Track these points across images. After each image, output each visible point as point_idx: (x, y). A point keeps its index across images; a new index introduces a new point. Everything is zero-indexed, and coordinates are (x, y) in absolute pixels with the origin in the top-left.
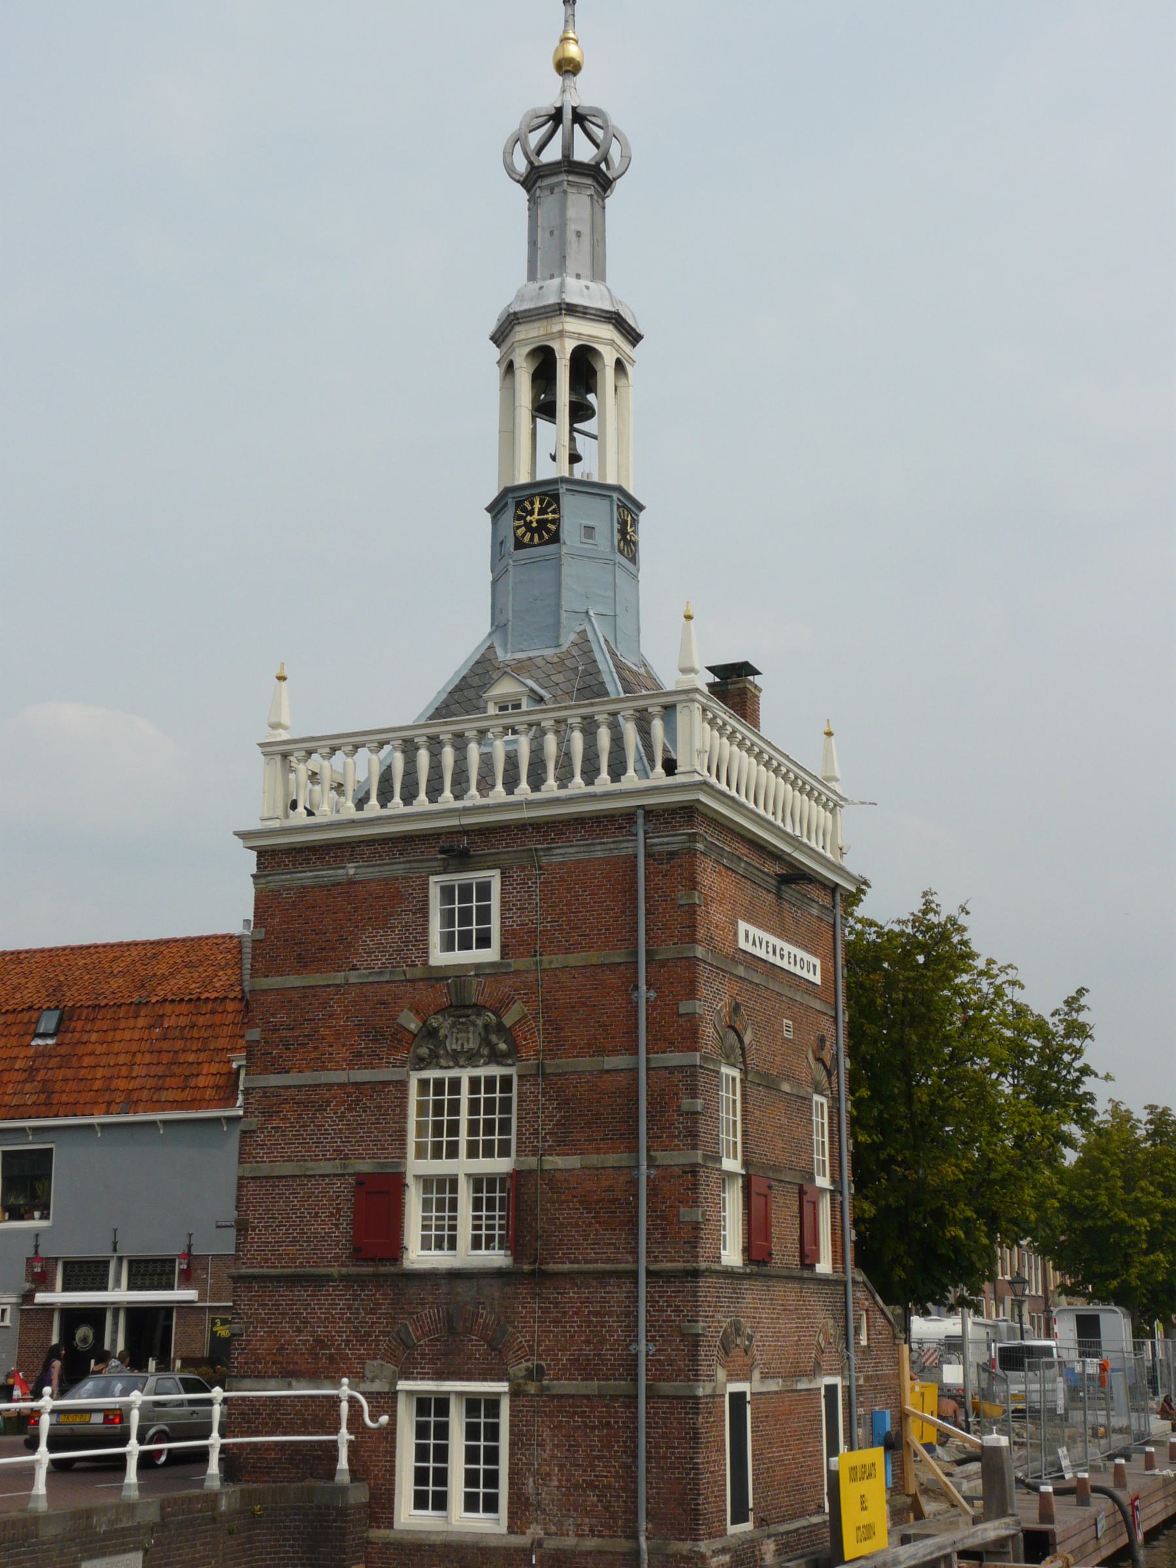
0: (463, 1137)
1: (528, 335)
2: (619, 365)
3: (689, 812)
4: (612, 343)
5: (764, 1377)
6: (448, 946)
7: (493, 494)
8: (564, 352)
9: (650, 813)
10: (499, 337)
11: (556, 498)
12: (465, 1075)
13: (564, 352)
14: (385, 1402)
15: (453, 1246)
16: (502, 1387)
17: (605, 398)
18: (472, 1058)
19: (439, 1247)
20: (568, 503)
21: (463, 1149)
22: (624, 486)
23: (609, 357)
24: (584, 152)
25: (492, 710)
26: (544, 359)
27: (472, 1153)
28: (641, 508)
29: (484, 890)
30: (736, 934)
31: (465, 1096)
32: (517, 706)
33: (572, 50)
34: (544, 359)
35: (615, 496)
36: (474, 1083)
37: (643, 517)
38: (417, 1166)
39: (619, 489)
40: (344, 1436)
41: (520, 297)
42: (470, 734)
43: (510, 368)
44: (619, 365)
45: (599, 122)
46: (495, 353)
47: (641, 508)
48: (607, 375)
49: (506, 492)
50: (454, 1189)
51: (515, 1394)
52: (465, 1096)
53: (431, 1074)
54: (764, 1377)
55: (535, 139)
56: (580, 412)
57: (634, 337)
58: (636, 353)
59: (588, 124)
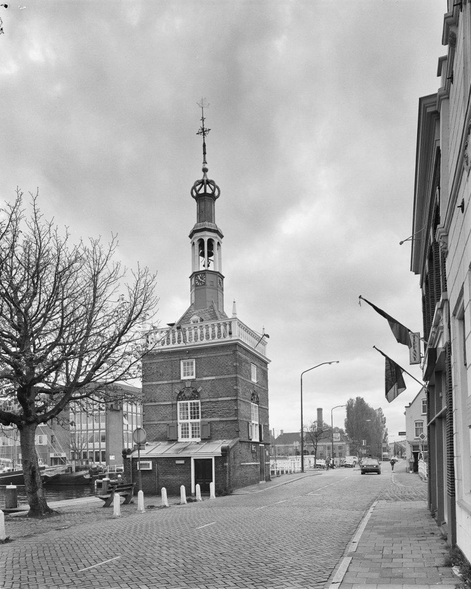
0: (189, 415)
1: (198, 235)
2: (219, 244)
3: (236, 344)
6: (185, 376)
7: (191, 274)
8: (206, 240)
10: (191, 236)
11: (204, 274)
12: (189, 402)
13: (206, 240)
15: (188, 437)
17: (215, 250)
18: (190, 399)
19: (185, 437)
20: (207, 275)
21: (189, 417)
22: (220, 272)
23: (216, 241)
24: (209, 191)
25: (192, 323)
26: (201, 242)
27: (191, 418)
28: (224, 277)
29: (192, 364)
31: (189, 407)
32: (197, 322)
34: (201, 242)
35: (218, 274)
36: (191, 403)
37: (224, 279)
38: (179, 421)
39: (218, 273)
41: (196, 226)
42: (187, 329)
43: (193, 244)
44: (219, 244)
45: (212, 183)
46: (190, 240)
47: (224, 277)
48: (215, 246)
49: (194, 273)
50: (188, 426)
52: (189, 407)
55: (198, 188)
56: (210, 254)
57: (222, 237)
58: (223, 240)
59: (210, 185)
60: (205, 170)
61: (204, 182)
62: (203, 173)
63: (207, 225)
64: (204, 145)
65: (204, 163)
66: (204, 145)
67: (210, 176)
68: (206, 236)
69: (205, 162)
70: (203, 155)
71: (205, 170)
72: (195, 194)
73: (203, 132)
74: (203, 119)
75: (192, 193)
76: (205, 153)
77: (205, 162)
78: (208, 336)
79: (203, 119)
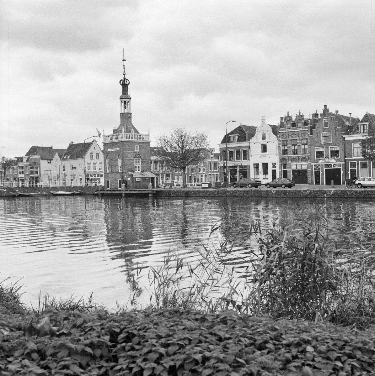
33: (124, 73)
63: (126, 96)
67: (127, 77)
68: (127, 100)
69: (124, 72)
71: (124, 75)
72: (121, 83)
73: (124, 60)
75: (120, 82)
76: (124, 68)
77: (124, 72)
78: (128, 135)
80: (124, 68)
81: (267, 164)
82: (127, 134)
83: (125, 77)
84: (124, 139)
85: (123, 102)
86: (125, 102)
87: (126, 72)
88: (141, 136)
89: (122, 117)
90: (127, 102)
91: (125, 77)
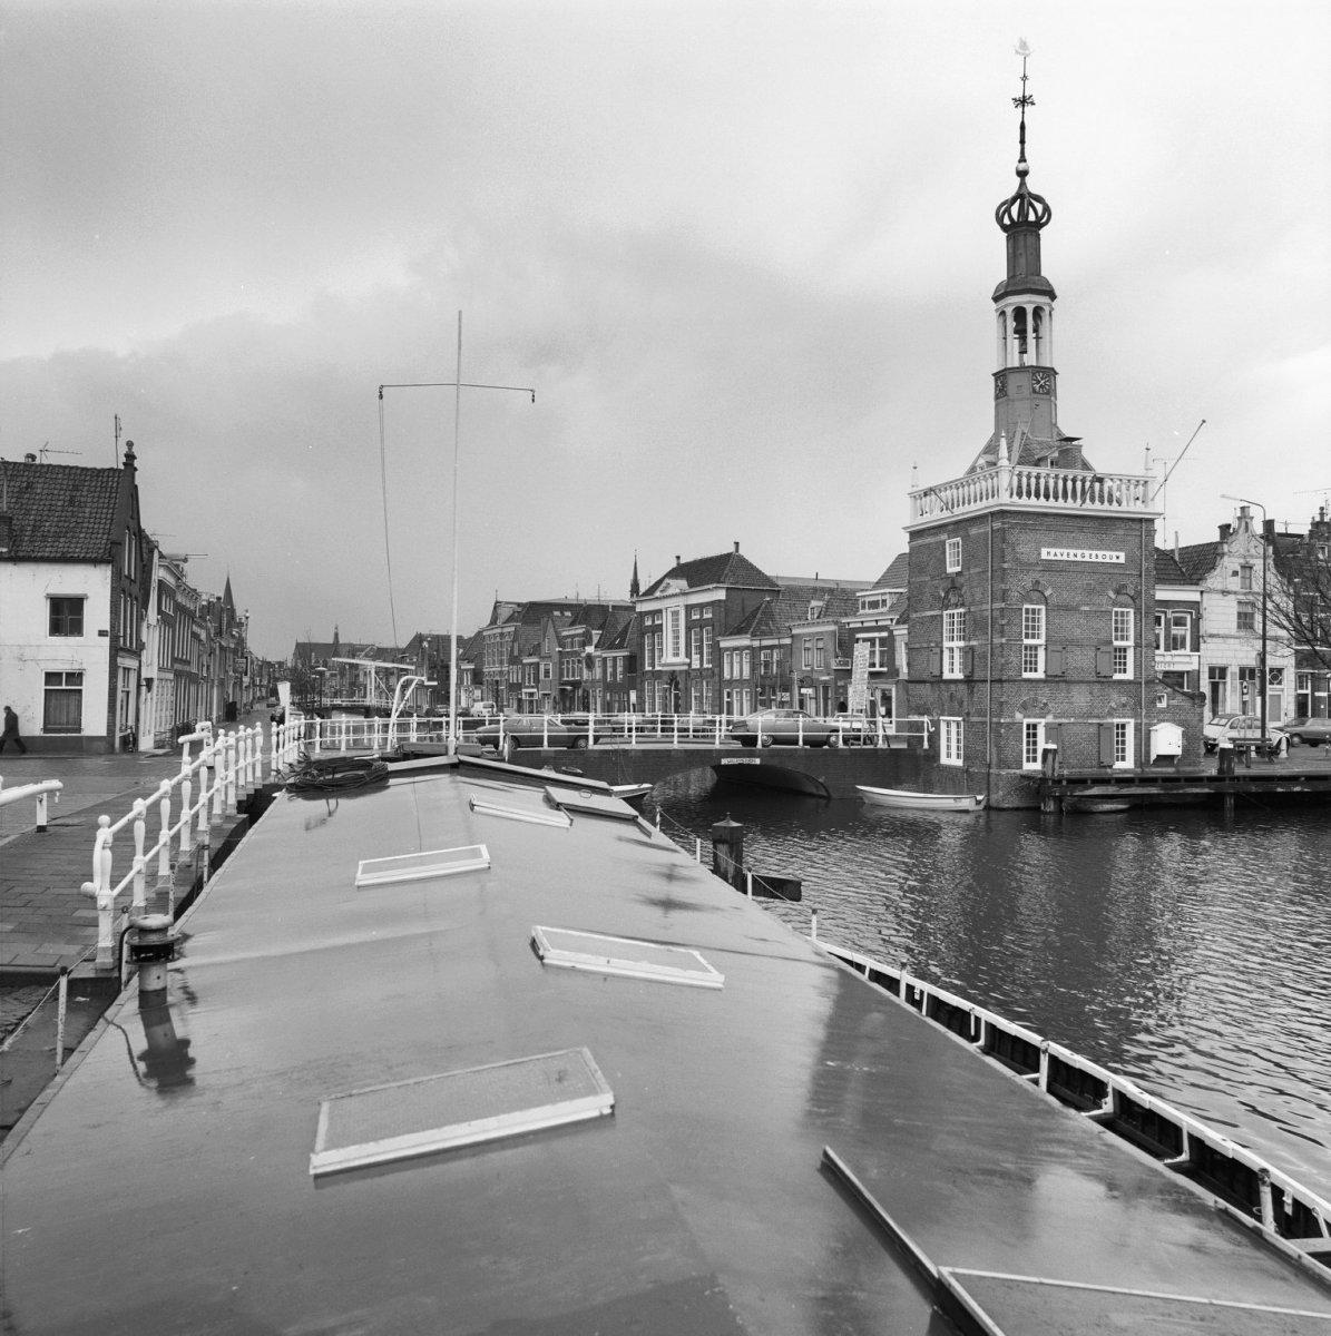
4: (1030, 302)
5: (1055, 717)
9: (992, 514)
12: (955, 611)
14: (936, 724)
16: (960, 719)
30: (1040, 554)
33: (1022, 166)
38: (946, 644)
40: (926, 734)
51: (964, 720)
53: (949, 612)
54: (1055, 717)
60: (1022, 174)
61: (1023, 197)
62: (1018, 180)
64: (1023, 127)
65: (1020, 161)
66: (1023, 127)
67: (1033, 185)
68: (1028, 302)
69: (1023, 159)
70: (1019, 146)
71: (1022, 174)
73: (1023, 102)
74: (1025, 78)
76: (1022, 142)
77: (1023, 159)
79: (1025, 78)
80: (1022, 142)
81: (1223, 671)
82: (1026, 469)
83: (1023, 184)
84: (1005, 500)
85: (1009, 311)
86: (1020, 313)
87: (1031, 164)
88: (1101, 480)
89: (1001, 392)
90: (1030, 309)
91: (1023, 184)
